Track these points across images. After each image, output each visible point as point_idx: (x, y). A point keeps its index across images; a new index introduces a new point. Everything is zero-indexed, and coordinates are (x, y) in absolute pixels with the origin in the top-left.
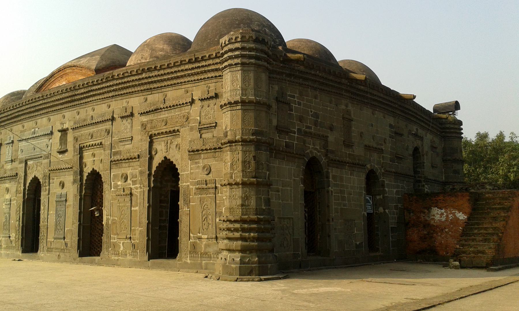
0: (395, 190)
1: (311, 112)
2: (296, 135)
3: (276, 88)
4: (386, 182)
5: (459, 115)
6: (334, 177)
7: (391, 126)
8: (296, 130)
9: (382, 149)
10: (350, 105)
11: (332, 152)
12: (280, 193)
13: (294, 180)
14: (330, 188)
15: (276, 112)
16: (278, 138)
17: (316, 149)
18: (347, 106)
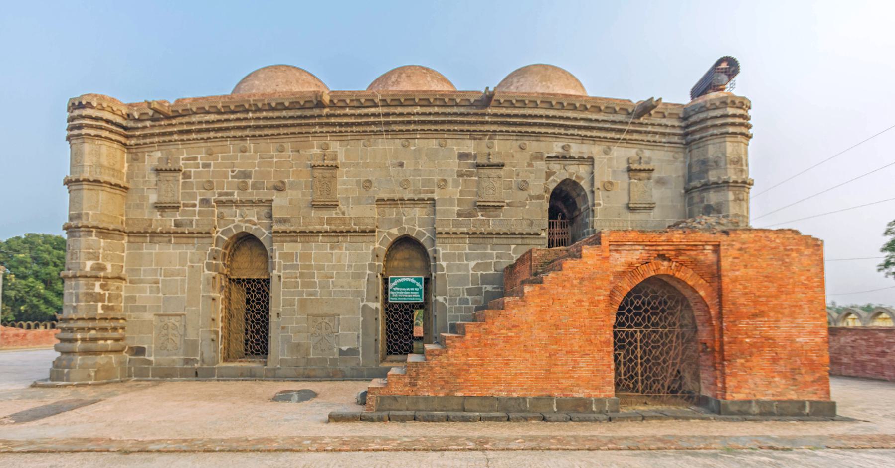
0: (472, 264)
1: (233, 172)
2: (197, 209)
3: (158, 154)
4: (441, 252)
5: (737, 88)
6: (284, 256)
7: (463, 156)
8: (197, 202)
9: (433, 200)
10: (335, 146)
11: (284, 221)
12: (160, 285)
13: (193, 267)
14: (275, 272)
15: (156, 185)
16: (159, 217)
17: (249, 221)
18: (325, 147)
